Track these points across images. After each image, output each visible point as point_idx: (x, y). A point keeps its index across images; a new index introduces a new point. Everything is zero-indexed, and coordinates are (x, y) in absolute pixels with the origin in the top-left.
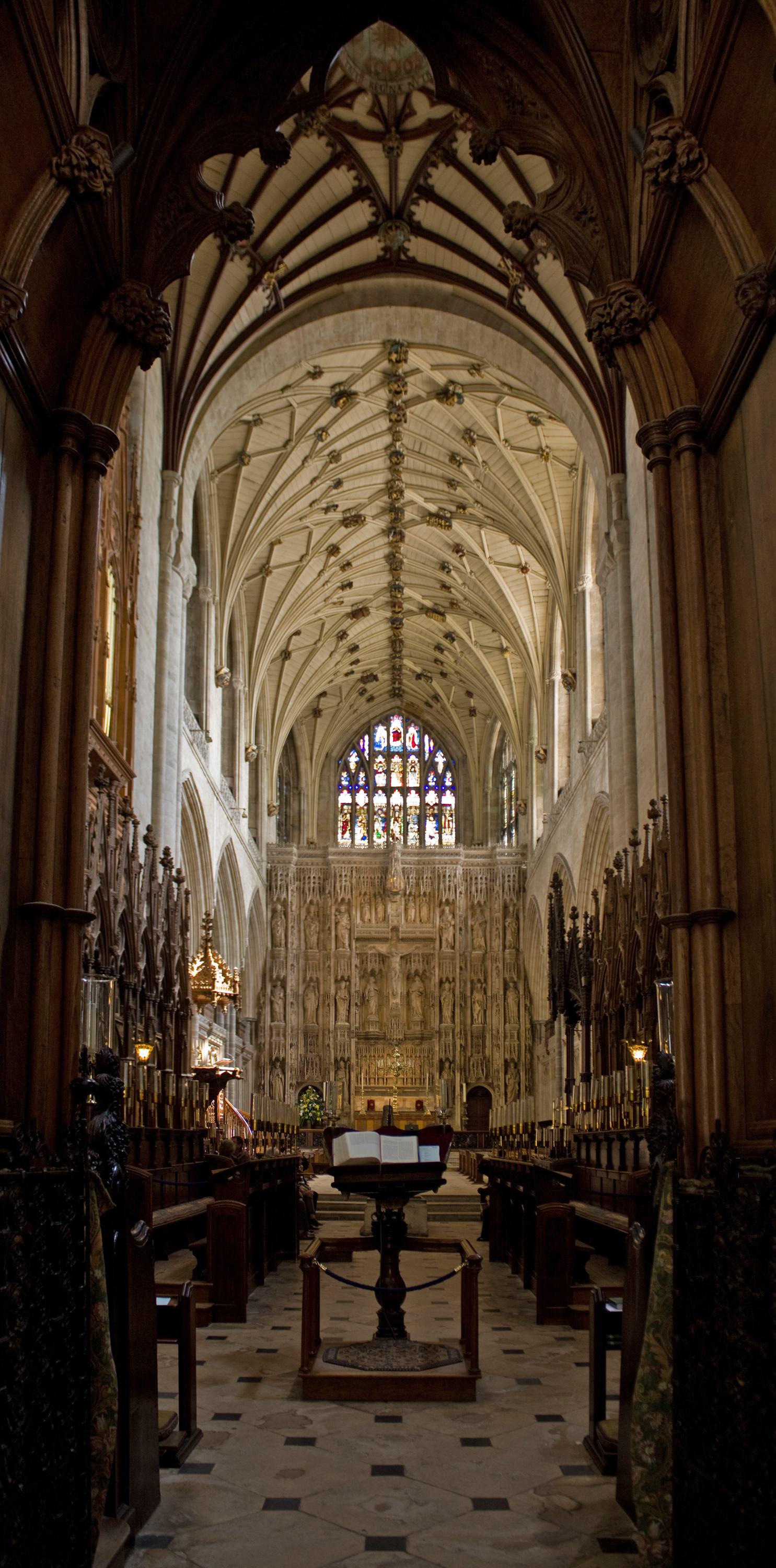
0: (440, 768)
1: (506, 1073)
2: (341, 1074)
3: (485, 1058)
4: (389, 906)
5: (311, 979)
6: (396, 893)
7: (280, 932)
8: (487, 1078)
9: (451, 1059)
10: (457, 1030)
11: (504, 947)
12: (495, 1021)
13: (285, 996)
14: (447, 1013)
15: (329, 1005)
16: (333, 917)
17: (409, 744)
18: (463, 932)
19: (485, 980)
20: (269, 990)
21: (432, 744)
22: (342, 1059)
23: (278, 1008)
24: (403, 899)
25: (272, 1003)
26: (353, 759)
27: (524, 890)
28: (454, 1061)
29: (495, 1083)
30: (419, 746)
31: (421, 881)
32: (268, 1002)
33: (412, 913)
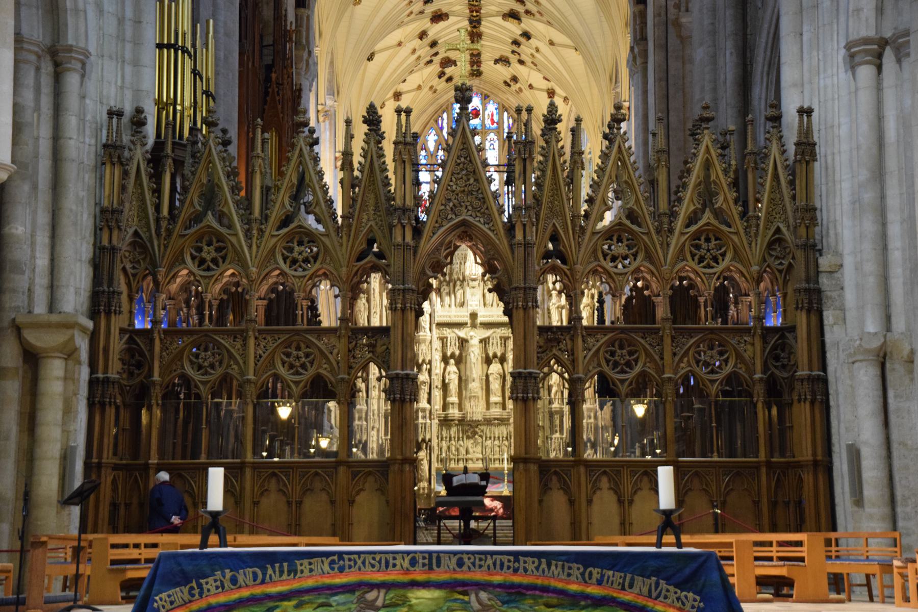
4: (468, 291)
17: (488, 122)
21: (511, 121)
22: (424, 440)
24: (482, 284)
30: (497, 124)
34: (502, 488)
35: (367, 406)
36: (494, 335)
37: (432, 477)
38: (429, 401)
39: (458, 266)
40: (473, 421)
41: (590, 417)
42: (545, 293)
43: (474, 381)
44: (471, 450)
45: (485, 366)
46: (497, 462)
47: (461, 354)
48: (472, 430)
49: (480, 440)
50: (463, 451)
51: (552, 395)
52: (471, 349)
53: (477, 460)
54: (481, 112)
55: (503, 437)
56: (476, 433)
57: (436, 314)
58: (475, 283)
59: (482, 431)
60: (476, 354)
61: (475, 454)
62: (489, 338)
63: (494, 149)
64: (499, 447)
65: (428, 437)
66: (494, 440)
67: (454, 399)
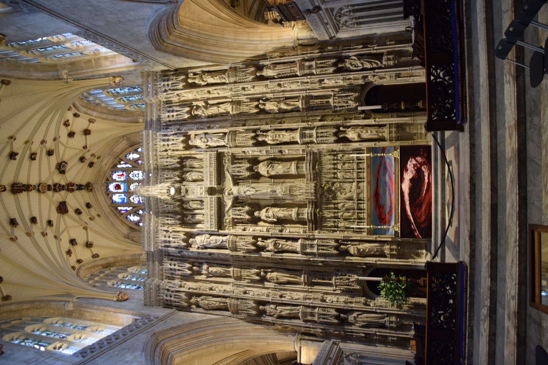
0: (136, 156)
2: (352, 249)
3: (334, 96)
4: (190, 196)
5: (258, 274)
6: (178, 191)
7: (214, 302)
8: (355, 92)
9: (334, 130)
10: (305, 125)
11: (224, 84)
12: (294, 87)
13: (273, 303)
14: (287, 137)
15: (282, 259)
16: (200, 250)
17: (123, 179)
18: (212, 126)
19: (258, 100)
21: (122, 162)
22: (336, 248)
23: (285, 311)
24: (184, 183)
25: (280, 317)
26: (134, 218)
27: (176, 70)
28: (337, 127)
29: (361, 82)
30: (123, 172)
32: (280, 321)
34: (391, 160)
35: (300, 305)
36: (230, 170)
37: (378, 239)
38: (295, 240)
39: (169, 206)
40: (315, 193)
42: (194, 121)
43: (275, 191)
44: (349, 195)
45: (262, 179)
46: (361, 166)
47: (249, 205)
48: (326, 194)
49: (337, 185)
50: (349, 204)
51: (289, 108)
53: (358, 187)
54: (117, 183)
55: (334, 160)
56: (329, 190)
57: (209, 229)
58: (183, 191)
59: (328, 182)
60: (248, 188)
61: (353, 190)
62: (233, 176)
63: (138, 174)
64: (344, 164)
65: (333, 243)
66: (337, 169)
67: (293, 213)
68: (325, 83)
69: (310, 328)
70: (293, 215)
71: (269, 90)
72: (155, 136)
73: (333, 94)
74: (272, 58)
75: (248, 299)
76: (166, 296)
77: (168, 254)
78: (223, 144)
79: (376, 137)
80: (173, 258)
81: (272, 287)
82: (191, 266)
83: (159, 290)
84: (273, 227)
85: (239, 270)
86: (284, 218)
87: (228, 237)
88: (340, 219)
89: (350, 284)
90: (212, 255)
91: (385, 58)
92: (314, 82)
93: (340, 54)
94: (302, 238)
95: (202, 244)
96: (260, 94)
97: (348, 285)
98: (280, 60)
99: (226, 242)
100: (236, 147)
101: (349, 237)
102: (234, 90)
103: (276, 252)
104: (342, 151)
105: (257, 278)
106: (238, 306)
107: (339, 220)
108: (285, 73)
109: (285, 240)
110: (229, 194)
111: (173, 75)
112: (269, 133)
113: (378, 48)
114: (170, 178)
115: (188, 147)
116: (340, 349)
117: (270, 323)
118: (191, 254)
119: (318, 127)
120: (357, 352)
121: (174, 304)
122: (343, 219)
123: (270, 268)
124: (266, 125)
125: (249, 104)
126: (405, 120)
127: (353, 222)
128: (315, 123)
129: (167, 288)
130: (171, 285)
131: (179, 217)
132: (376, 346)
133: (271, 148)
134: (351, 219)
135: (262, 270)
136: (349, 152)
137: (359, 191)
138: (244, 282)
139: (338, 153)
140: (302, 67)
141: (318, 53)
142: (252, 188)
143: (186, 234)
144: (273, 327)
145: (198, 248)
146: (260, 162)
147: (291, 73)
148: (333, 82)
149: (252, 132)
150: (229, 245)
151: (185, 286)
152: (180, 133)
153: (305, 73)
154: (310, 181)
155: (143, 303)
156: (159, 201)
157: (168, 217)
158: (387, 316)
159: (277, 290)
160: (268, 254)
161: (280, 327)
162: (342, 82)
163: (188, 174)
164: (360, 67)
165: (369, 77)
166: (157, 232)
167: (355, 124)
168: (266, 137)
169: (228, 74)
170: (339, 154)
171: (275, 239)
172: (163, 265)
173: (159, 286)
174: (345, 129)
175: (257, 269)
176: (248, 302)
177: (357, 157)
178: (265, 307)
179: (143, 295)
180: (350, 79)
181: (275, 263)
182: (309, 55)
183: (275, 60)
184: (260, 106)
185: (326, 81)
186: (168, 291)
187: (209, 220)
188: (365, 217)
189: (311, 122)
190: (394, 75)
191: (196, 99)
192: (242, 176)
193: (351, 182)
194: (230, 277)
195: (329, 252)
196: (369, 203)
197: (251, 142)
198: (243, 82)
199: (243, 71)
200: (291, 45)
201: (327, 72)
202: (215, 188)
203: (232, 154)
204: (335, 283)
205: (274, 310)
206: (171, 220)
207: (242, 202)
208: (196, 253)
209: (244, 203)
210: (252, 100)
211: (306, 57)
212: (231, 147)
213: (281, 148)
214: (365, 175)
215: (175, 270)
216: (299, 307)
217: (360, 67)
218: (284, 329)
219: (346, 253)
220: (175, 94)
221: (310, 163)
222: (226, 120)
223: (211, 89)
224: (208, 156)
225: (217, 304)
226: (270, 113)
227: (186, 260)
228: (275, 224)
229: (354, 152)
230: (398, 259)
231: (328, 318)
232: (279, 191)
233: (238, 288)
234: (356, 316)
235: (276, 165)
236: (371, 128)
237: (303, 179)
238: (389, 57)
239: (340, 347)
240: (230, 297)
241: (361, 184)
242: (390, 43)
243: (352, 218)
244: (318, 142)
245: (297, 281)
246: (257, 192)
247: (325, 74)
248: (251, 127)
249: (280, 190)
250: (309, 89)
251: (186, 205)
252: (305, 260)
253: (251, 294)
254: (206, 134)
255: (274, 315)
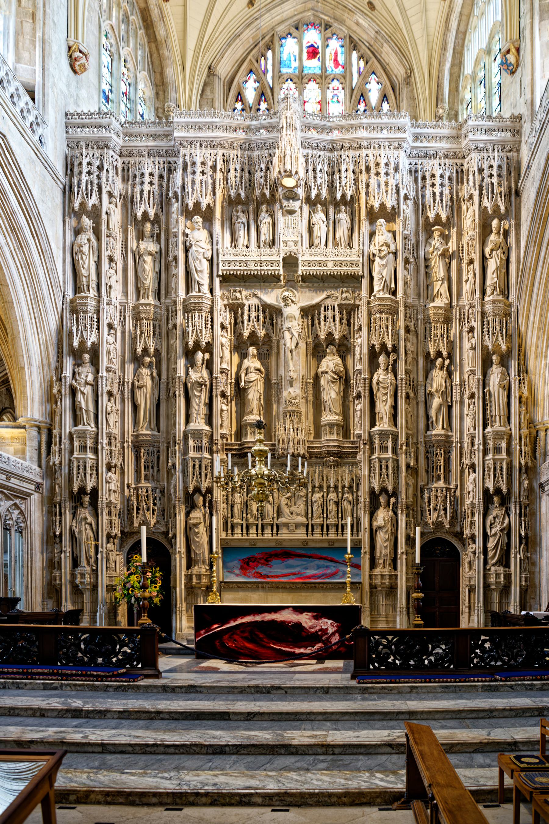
1: (485, 515)
4: (281, 220)
5: (145, 351)
9: (390, 489)
10: (402, 438)
11: (483, 292)
12: (468, 421)
15: (175, 395)
19: (450, 356)
20: (68, 372)
22: (197, 490)
24: (306, 209)
25: (73, 392)
27: (518, 194)
28: (395, 494)
29: (467, 532)
31: (337, 176)
32: (66, 390)
33: (321, 231)
35: (97, 427)
38: (209, 421)
39: (263, 174)
41: (497, 450)
44: (286, 510)
47: (267, 336)
52: (287, 325)
53: (297, 526)
55: (343, 487)
57: (221, 258)
60: (296, 335)
61: (294, 516)
62: (317, 306)
68: (469, 474)
69: (60, 444)
70: (252, 417)
71: (465, 376)
72: (396, 145)
73: (451, 487)
74: (520, 383)
75: (99, 332)
76: (89, 164)
77: (172, 168)
78: (376, 288)
79: (378, 554)
80: (166, 180)
81: (126, 377)
82: (152, 219)
83: (98, 148)
84: (229, 381)
85: (151, 315)
86: (246, 400)
87: (209, 295)
88: (247, 496)
89: (141, 512)
90: (174, 264)
91: (501, 569)
92: (473, 456)
93: (513, 500)
94: (212, 432)
95: (193, 242)
96: (461, 360)
97: (138, 509)
98: (515, 397)
99: (200, 291)
100: (370, 314)
101: (217, 511)
102: (470, 311)
103: (185, 385)
104: (358, 500)
105: (139, 350)
106: (83, 312)
107: (245, 494)
108: (491, 407)
109: (207, 401)
110: (285, 299)
111: (510, 188)
112: (391, 376)
113: (518, 560)
114: (315, 178)
115: (372, 217)
116: (29, 495)
117: (62, 373)
118: (173, 220)
119: (397, 461)
120: (29, 523)
121: (75, 180)
122: (247, 502)
123: (159, 375)
124: (406, 370)
125: (445, 339)
126: (401, 598)
127: (243, 518)
128: (404, 456)
129: (106, 167)
130: (111, 175)
131: (243, 195)
132: (42, 553)
133: (365, 379)
134: (247, 514)
135: (154, 359)
136: (355, 512)
137: (292, 528)
138: (129, 324)
139: (355, 495)
140: (498, 436)
141: (520, 463)
142: (297, 344)
143: (210, 209)
144: (55, 379)
145: (187, 235)
146: (343, 358)
147: (492, 416)
148: (471, 488)
149: (394, 346)
150: (194, 297)
151: (113, 206)
152: (398, 200)
153: (489, 441)
154: (309, 447)
155: (72, 111)
156: (271, 151)
157: (242, 170)
158: (93, 570)
159: (121, 386)
160: (181, 372)
161: (55, 390)
162: (469, 502)
163: (322, 216)
164: (491, 531)
165: (474, 546)
166: (213, 147)
167: (400, 521)
168: (384, 370)
169: (499, 301)
170: (353, 495)
171: (208, 383)
172: (149, 157)
173: (107, 147)
174: (391, 505)
175: (156, 350)
176: (94, 333)
177: (346, 524)
178: (88, 365)
179: (86, 111)
180: (473, 514)
181: (168, 383)
182: (518, 447)
183: (515, 388)
184: (440, 360)
185: (473, 476)
186: (98, 167)
187: (238, 258)
188: (251, 537)
189: (406, 450)
190: (472, 583)
191: (462, 235)
192: (319, 323)
193: (307, 514)
194: (138, 298)
195: (191, 478)
196: (273, 544)
197: (376, 342)
198: (483, 329)
199: (501, 330)
200: (538, 418)
201: (487, 477)
202: (297, 272)
203: (358, 306)
204: (141, 488)
205: (83, 382)
206: (236, 177)
207: (272, 324)
208: (175, 230)
209: (271, 327)
210: (451, 345)
211: (515, 443)
212: (369, 303)
213: (365, 396)
214: (317, 537)
215: (142, 183)
216: (93, 425)
217: (491, 531)
218: (53, 399)
219: (191, 506)
220: (473, 191)
221: (338, 447)
222: (419, 295)
223: (477, 265)
224: (354, 258)
225: (84, 272)
226: (426, 378)
227: (162, 208)
228: (235, 384)
229: (355, 520)
230: (185, 586)
231: (80, 475)
232: (292, 393)
233: (118, 315)
234: (89, 521)
235: (336, 388)
236: (392, 547)
237: (313, 436)
238: (502, 576)
239: (32, 494)
240: (99, 296)
241: (303, 530)
242: (524, 579)
243: (249, 516)
244: (372, 462)
245: (139, 422)
246: (289, 353)
247: (484, 475)
248: (402, 343)
249: (293, 394)
250: (461, 448)
251: (264, 210)
252: (175, 437)
253: (109, 337)
254: (395, 254)
255: (76, 381)
